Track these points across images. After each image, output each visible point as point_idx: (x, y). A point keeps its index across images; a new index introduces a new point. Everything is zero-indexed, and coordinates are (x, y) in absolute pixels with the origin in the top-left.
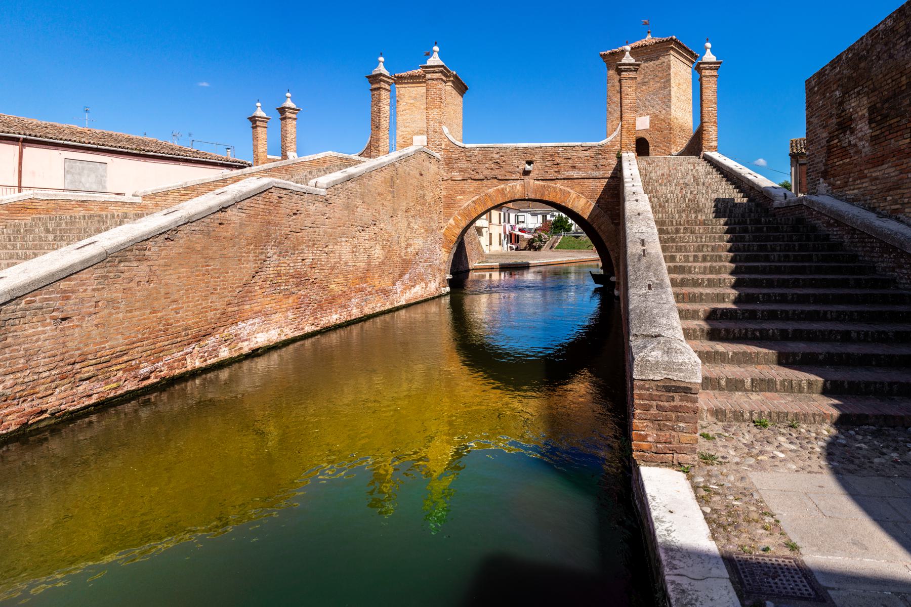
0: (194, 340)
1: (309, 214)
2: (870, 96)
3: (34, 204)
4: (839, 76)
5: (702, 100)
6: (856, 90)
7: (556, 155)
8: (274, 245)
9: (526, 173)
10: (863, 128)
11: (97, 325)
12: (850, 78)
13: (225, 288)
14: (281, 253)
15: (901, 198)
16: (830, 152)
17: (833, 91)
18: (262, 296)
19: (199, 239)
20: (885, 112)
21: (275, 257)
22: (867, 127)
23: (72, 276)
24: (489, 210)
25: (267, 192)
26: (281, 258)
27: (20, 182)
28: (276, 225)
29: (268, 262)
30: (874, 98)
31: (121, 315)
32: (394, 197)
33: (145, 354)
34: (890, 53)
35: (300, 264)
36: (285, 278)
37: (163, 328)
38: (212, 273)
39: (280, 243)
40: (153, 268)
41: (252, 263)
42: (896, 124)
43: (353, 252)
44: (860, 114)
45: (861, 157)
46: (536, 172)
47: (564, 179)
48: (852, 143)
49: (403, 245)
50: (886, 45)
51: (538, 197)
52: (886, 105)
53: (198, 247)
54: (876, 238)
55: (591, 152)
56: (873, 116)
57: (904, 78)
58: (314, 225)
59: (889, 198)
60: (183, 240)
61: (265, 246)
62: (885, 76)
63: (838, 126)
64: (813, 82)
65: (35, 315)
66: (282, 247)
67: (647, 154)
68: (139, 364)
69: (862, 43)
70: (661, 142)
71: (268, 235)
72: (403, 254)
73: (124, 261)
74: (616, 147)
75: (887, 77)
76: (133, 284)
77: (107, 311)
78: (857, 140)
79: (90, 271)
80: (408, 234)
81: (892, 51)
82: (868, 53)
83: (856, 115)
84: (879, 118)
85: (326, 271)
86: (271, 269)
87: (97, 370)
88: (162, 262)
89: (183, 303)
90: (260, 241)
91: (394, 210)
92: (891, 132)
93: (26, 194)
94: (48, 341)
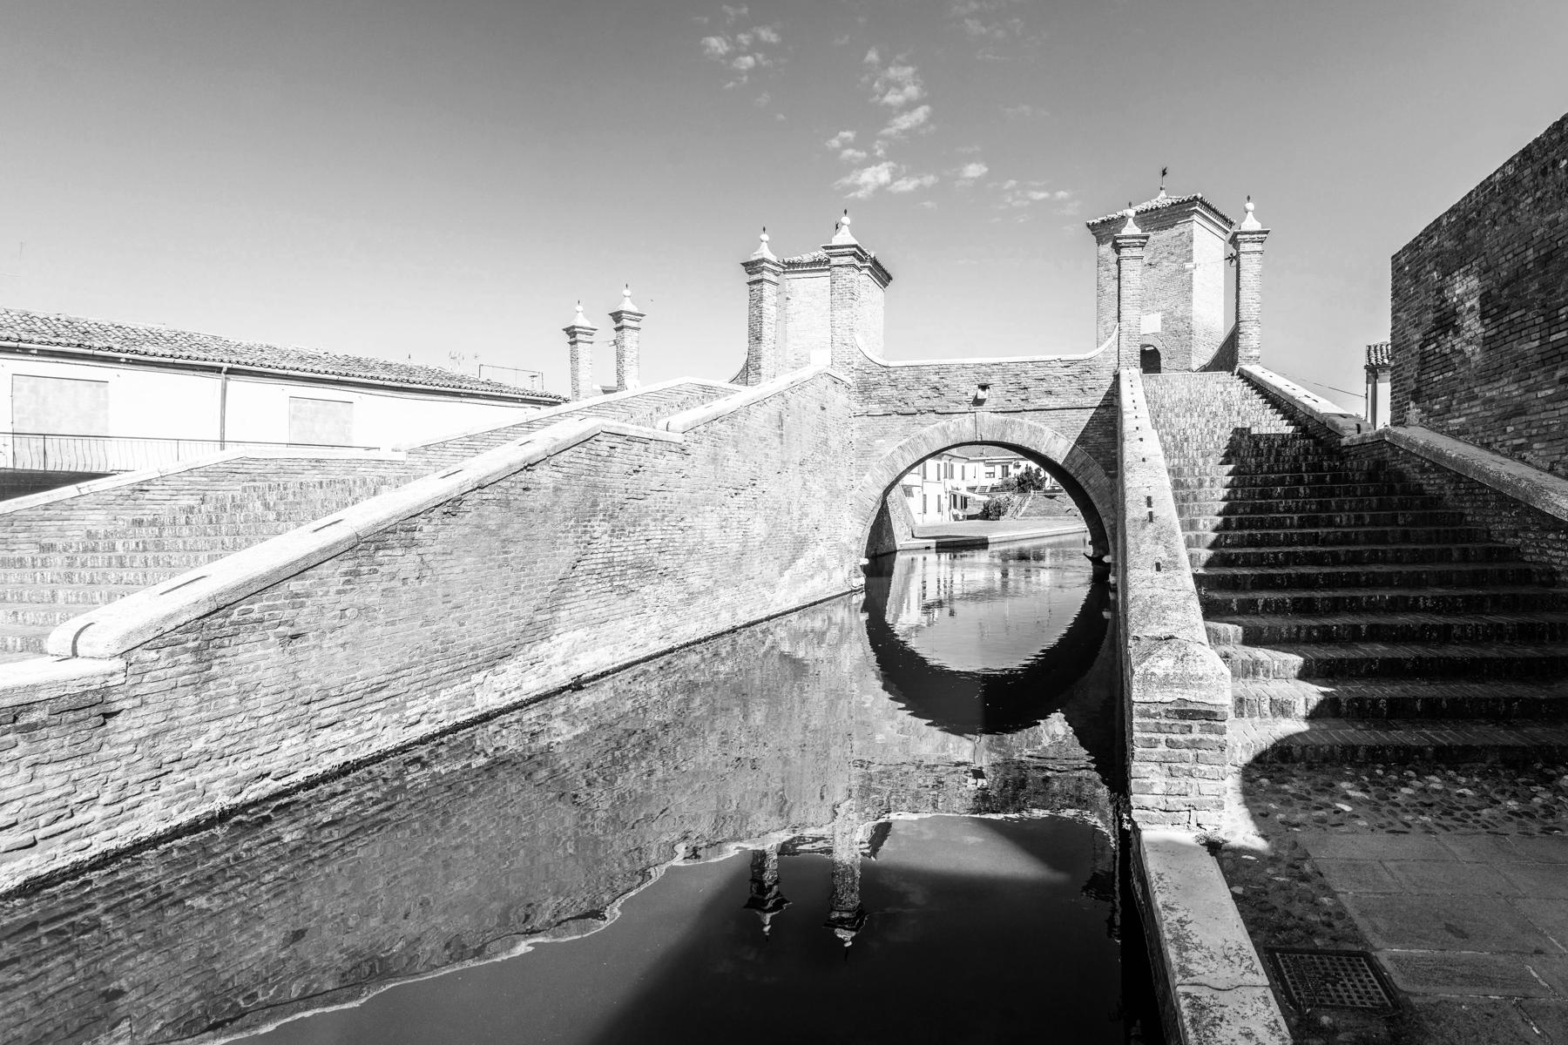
0: (486, 664)
1: (656, 471)
2: (1483, 278)
3: (246, 466)
4: (1437, 250)
5: (1238, 289)
6: (1461, 270)
7: (1023, 375)
8: (604, 520)
9: (978, 402)
10: (1473, 326)
11: (343, 645)
12: (1453, 252)
13: (532, 586)
14: (613, 531)
15: (1526, 428)
16: (1426, 363)
17: (1429, 272)
18: (585, 597)
19: (492, 512)
20: (1503, 301)
21: (606, 538)
22: (1477, 325)
23: (307, 573)
24: (922, 460)
25: (592, 440)
26: (614, 540)
27: (223, 434)
28: (605, 489)
29: (595, 546)
30: (1488, 282)
31: (378, 630)
32: (782, 443)
33: (414, 687)
34: (1511, 215)
35: (644, 546)
36: (620, 568)
37: (440, 647)
38: (512, 563)
39: (611, 516)
40: (426, 558)
41: (571, 548)
42: (1519, 320)
43: (722, 527)
44: (1468, 305)
45: (1469, 369)
46: (994, 401)
47: (1035, 410)
48: (1456, 348)
49: (796, 515)
50: (1504, 203)
51: (996, 438)
52: (1506, 291)
53: (492, 524)
54: (1490, 488)
55: (1075, 370)
56: (1488, 307)
57: (1531, 251)
58: (664, 488)
59: (1509, 429)
60: (470, 514)
61: (589, 521)
62: (1503, 249)
63: (1437, 323)
64: (1403, 259)
65: (254, 630)
66: (614, 522)
67: (1158, 370)
68: (405, 702)
69: (1471, 201)
70: (1178, 351)
71: (595, 504)
72: (795, 529)
73: (383, 549)
74: (1111, 361)
75: (1506, 250)
76: (397, 583)
77: (357, 623)
78: (1464, 344)
79: (333, 565)
80: (803, 499)
81: (1513, 212)
82: (1479, 215)
83: (1462, 307)
84: (1495, 310)
85: (681, 557)
86: (600, 556)
87: (344, 712)
88: (438, 548)
89: (469, 610)
90: (585, 513)
91: (783, 462)
92: (1513, 330)
93: (232, 452)
94: (271, 670)
